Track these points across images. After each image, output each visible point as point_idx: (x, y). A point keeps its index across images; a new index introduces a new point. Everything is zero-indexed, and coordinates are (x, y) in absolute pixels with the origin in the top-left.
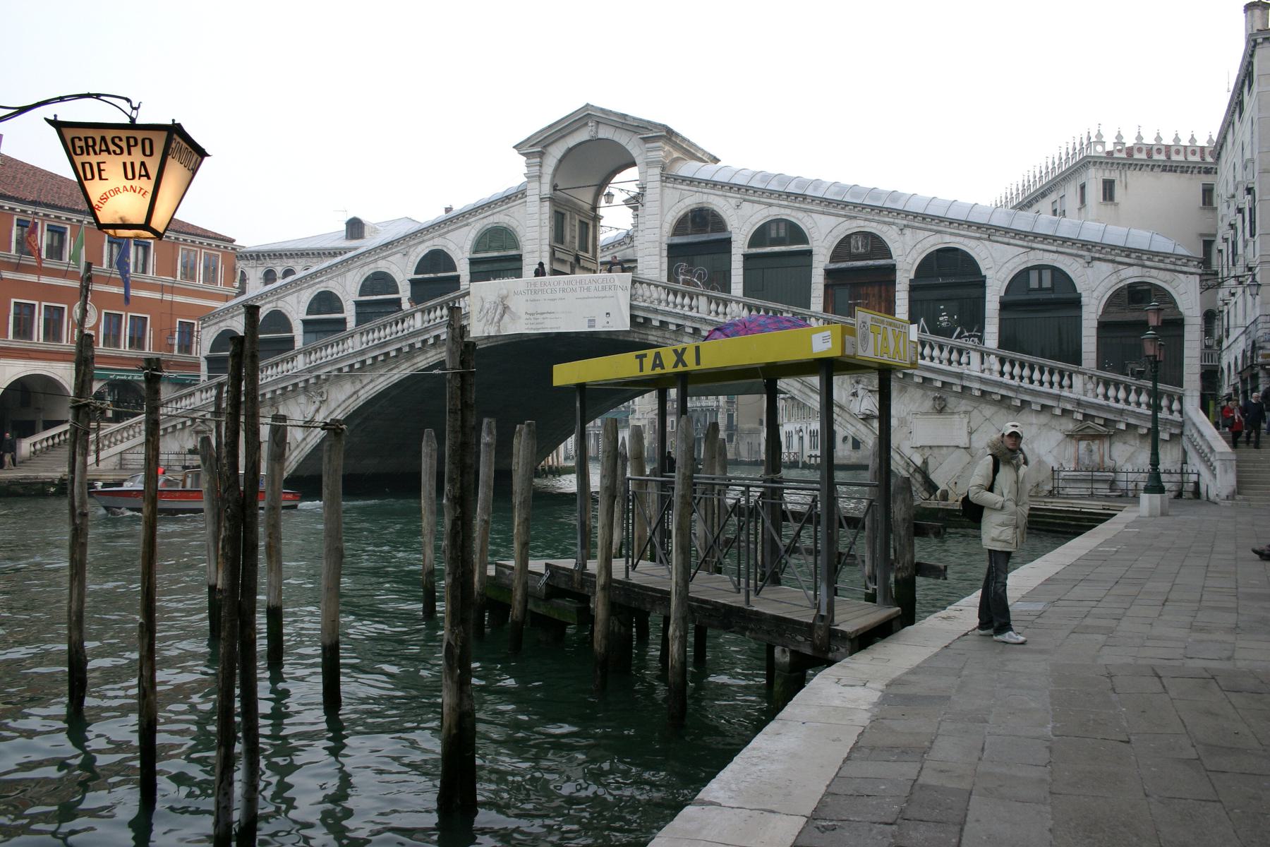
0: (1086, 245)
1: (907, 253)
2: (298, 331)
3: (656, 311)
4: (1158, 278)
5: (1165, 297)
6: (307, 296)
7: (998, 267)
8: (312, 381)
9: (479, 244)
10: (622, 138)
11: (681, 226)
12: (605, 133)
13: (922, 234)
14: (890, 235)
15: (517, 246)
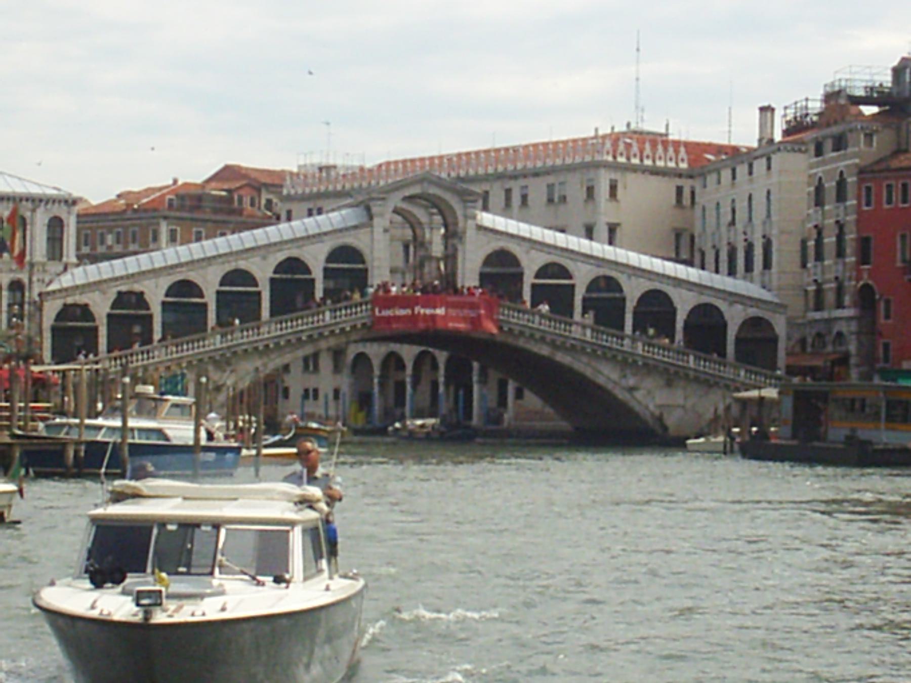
0: (731, 294)
1: (633, 290)
2: (156, 311)
3: (510, 323)
4: (766, 315)
5: (769, 325)
6: (165, 282)
7: (684, 304)
8: (228, 355)
9: (331, 257)
10: (447, 196)
11: (489, 260)
12: (433, 190)
13: (642, 280)
14: (622, 279)
15: (363, 262)
